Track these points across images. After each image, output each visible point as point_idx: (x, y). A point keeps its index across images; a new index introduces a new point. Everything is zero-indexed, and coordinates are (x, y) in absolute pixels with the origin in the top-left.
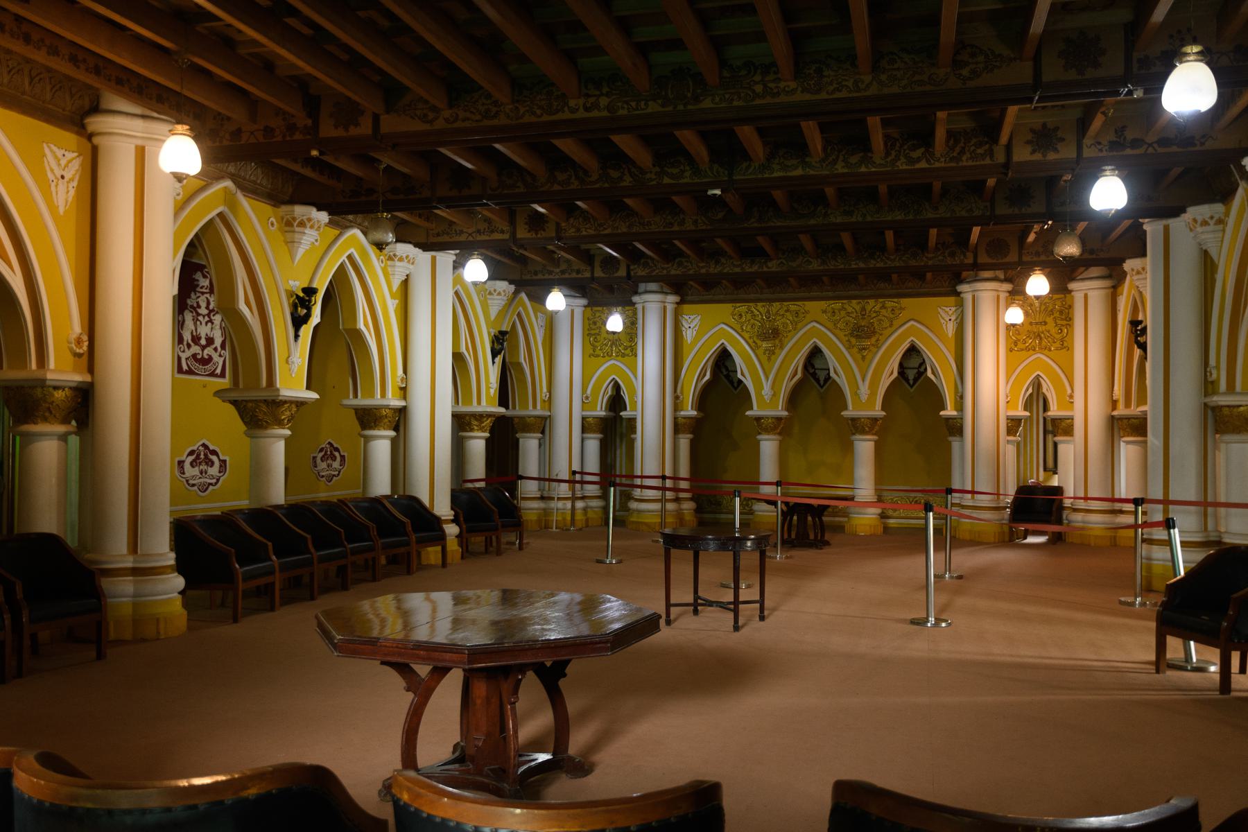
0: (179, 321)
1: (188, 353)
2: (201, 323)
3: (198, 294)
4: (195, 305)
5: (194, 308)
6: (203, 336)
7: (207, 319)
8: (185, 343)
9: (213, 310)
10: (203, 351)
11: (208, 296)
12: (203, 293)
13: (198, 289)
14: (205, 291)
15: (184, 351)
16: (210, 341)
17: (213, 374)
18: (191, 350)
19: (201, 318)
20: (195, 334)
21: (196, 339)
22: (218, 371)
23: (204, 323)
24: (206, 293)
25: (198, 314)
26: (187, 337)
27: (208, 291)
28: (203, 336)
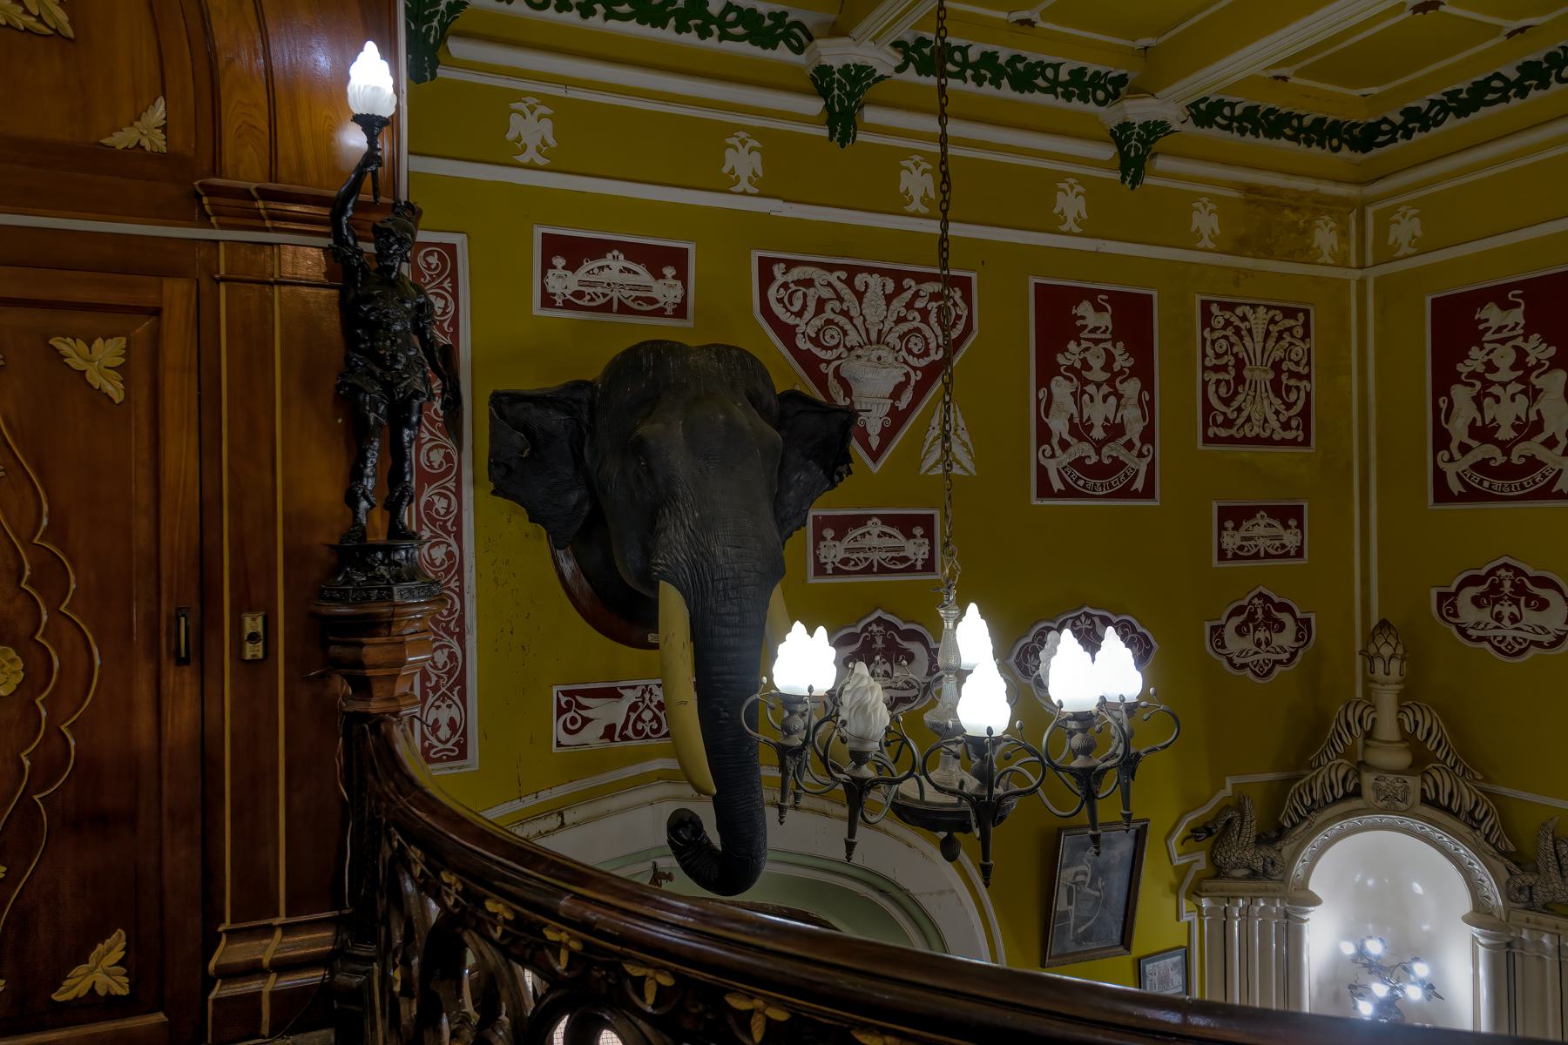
0: (1038, 402)
2: (1092, 399)
3: (1084, 344)
4: (1078, 365)
5: (1077, 373)
6: (1098, 421)
7: (1105, 389)
10: (1098, 452)
11: (1108, 345)
12: (1097, 342)
14: (1103, 336)
16: (1115, 430)
17: (1125, 493)
18: (1071, 450)
19: (1091, 389)
20: (1077, 420)
22: (1139, 484)
23: (1098, 398)
24: (1106, 340)
25: (1086, 382)
26: (1059, 425)
27: (1108, 336)
28: (1098, 421)
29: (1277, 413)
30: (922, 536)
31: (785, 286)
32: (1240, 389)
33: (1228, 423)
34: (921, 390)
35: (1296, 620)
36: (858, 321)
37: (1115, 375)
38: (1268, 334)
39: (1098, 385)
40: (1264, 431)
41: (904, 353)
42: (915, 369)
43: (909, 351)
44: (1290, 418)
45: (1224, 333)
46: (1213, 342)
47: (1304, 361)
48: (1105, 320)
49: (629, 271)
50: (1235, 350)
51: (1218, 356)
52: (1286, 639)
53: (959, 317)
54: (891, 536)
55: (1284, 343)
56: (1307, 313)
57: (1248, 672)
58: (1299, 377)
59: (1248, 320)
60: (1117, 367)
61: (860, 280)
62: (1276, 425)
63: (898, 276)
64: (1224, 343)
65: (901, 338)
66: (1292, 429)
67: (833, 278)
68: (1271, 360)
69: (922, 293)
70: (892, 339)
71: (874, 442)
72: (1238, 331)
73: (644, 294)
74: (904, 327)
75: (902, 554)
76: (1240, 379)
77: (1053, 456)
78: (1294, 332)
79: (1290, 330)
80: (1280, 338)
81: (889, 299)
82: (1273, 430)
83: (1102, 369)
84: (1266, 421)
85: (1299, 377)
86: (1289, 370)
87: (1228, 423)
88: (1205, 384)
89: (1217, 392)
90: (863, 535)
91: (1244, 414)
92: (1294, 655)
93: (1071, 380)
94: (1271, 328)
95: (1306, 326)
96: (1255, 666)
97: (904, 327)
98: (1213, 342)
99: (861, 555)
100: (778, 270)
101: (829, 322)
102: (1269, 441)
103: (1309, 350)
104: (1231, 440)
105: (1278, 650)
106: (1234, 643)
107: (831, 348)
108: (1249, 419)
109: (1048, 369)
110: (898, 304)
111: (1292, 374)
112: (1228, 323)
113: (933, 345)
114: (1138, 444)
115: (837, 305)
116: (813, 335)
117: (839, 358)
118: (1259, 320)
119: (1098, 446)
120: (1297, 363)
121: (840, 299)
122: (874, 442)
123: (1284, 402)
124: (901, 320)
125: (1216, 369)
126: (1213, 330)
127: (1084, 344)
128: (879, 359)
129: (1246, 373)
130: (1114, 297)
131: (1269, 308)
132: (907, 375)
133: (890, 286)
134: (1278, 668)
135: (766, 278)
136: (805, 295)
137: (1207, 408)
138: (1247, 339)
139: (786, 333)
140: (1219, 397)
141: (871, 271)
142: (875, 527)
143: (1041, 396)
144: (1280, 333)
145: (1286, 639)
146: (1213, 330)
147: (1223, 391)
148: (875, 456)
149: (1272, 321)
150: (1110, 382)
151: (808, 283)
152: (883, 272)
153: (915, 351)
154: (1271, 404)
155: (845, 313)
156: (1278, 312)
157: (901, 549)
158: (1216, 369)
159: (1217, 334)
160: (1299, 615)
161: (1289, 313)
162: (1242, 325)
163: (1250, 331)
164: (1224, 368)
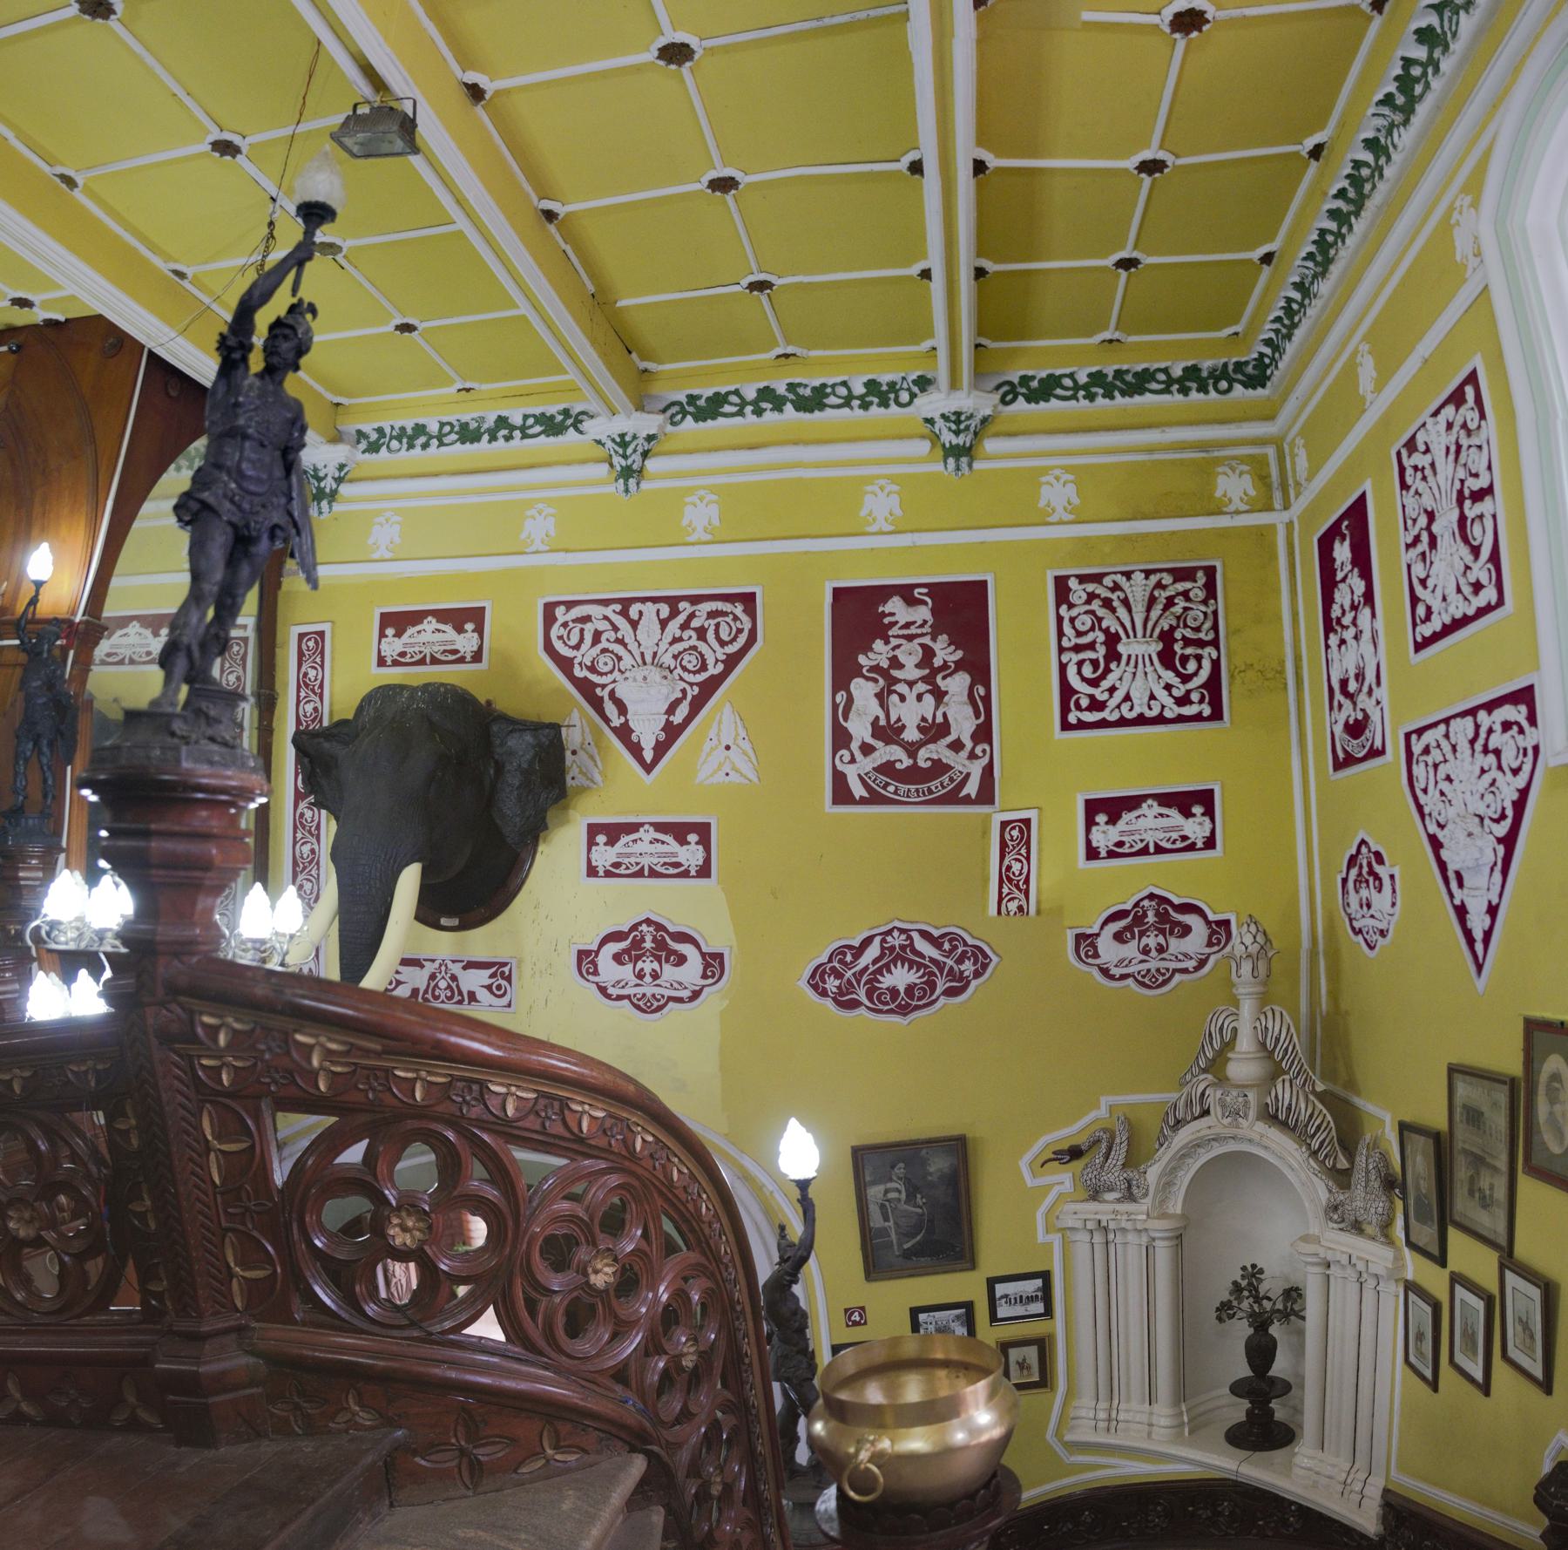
0: (835, 706)
1: (867, 764)
2: (903, 698)
3: (894, 642)
4: (885, 664)
8: (855, 746)
12: (910, 638)
13: (894, 631)
15: (853, 761)
20: (882, 722)
21: (887, 732)
23: (911, 697)
26: (859, 729)
29: (1168, 687)
30: (697, 843)
31: (565, 625)
32: (1113, 666)
33: (1096, 705)
34: (697, 705)
35: (1208, 923)
36: (632, 646)
38: (1152, 601)
39: (911, 684)
40: (1150, 709)
41: (679, 670)
42: (691, 684)
43: (684, 669)
44: (1188, 692)
45: (1087, 607)
46: (1072, 620)
47: (1208, 625)
48: (923, 613)
49: (439, 631)
50: (1104, 625)
51: (1079, 634)
52: (1196, 941)
53: (740, 631)
54: (663, 843)
56: (1210, 572)
57: (1130, 981)
58: (1201, 644)
59: (1121, 590)
61: (634, 611)
62: (1169, 702)
63: (673, 602)
64: (1088, 620)
65: (675, 657)
66: (1191, 703)
67: (608, 611)
68: (1157, 631)
69: (697, 613)
70: (667, 660)
71: (648, 755)
72: (1107, 603)
73: (448, 648)
74: (679, 647)
75: (674, 860)
76: (1113, 655)
77: (853, 761)
78: (1191, 594)
79: (1185, 595)
80: (1170, 603)
81: (664, 624)
82: (1163, 707)
83: (917, 666)
84: (1152, 697)
85: (1201, 644)
86: (1184, 638)
87: (1096, 705)
88: (1063, 668)
89: (1079, 673)
90: (635, 841)
91: (1119, 695)
92: (1202, 963)
93: (876, 681)
94: (1156, 593)
95: (1210, 587)
96: (1144, 977)
97: (679, 647)
98: (1072, 620)
99: (633, 860)
100: (560, 611)
101: (604, 651)
102: (1160, 720)
103: (1215, 613)
104: (1103, 724)
105: (1180, 957)
106: (1109, 951)
107: (606, 674)
108: (1127, 698)
109: (844, 673)
110: (673, 627)
111: (1187, 642)
112: (1091, 597)
113: (710, 661)
115: (612, 635)
116: (589, 664)
117: (614, 681)
118: (1138, 589)
120: (1198, 630)
121: (616, 629)
122: (648, 755)
123: (1178, 674)
124: (675, 640)
125: (1077, 649)
126: (1071, 606)
127: (894, 642)
128: (645, 678)
129: (1121, 648)
130: (935, 590)
131: (1148, 573)
132: (684, 691)
133: (665, 611)
134: (1178, 977)
135: (549, 619)
136: (582, 631)
137: (1067, 691)
138: (1122, 612)
139: (565, 665)
140: (1084, 679)
141: (644, 600)
142: (647, 834)
143: (838, 699)
144: (1170, 603)
145: (1196, 941)
146: (1071, 606)
147: (1087, 671)
148: (648, 768)
151: (586, 619)
152: (655, 600)
153: (690, 667)
154: (1160, 677)
155: (620, 642)
156: (1164, 575)
157: (674, 855)
158: (1077, 649)
159: (1074, 612)
160: (1211, 917)
162: (1114, 596)
163: (1126, 603)
164: (1091, 646)
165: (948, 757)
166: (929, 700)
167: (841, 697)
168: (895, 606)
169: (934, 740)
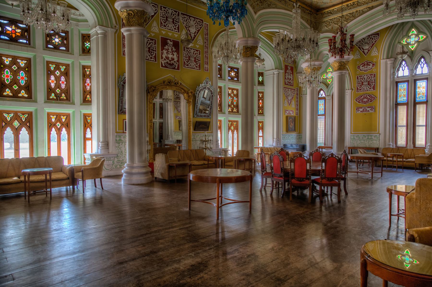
0: (161, 53)
1: (165, 61)
5: (167, 50)
8: (164, 59)
9: (174, 51)
10: (170, 62)
12: (170, 46)
13: (168, 45)
16: (173, 59)
21: (167, 58)
22: (176, 68)
23: (170, 54)
25: (168, 51)
26: (164, 56)
37: (173, 51)
55: (196, 55)
60: (173, 50)
72: (189, 52)
85: (198, 60)
114: (176, 62)
118: (192, 51)
119: (170, 61)
131: (194, 49)
149: (194, 51)
150: (172, 52)
161: (197, 51)
165: (174, 63)
166: (172, 55)
167: (162, 52)
168: (168, 41)
169: (172, 60)
